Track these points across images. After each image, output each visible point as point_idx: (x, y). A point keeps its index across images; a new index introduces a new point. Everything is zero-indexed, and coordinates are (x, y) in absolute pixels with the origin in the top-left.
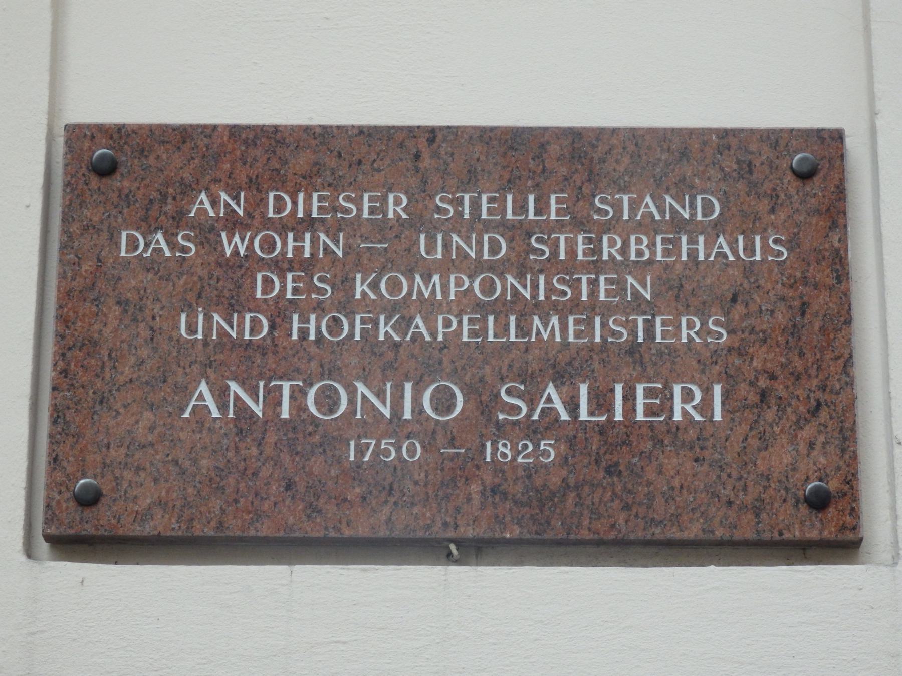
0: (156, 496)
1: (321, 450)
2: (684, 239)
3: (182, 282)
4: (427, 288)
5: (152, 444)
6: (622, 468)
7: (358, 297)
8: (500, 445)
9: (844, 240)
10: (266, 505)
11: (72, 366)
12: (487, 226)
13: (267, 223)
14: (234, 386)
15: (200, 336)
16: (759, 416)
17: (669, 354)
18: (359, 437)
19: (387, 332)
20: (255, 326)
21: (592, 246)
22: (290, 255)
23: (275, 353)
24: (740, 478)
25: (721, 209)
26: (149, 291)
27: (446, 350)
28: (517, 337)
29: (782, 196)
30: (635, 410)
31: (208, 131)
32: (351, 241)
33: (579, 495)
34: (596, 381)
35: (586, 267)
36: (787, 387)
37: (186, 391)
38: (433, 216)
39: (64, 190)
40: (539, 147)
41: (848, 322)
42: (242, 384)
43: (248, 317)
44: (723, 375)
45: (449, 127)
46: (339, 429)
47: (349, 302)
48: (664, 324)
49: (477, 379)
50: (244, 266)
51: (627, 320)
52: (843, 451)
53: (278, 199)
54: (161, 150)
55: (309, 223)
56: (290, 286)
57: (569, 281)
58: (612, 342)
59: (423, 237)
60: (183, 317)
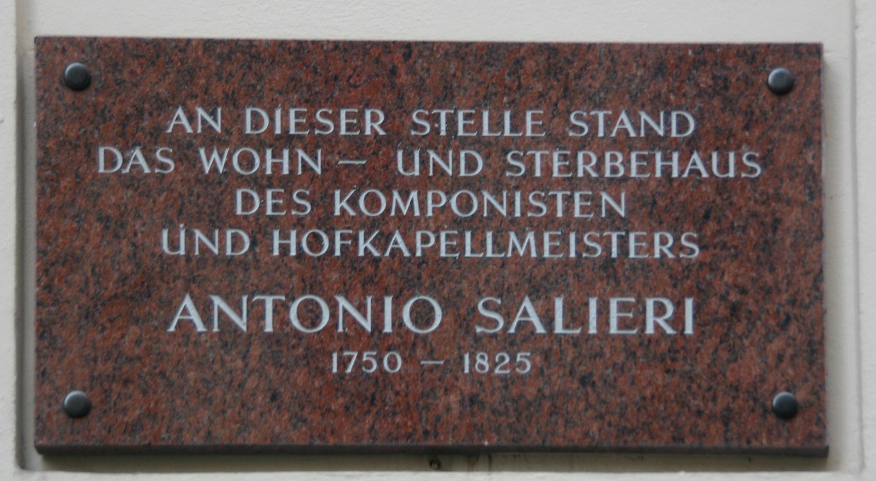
0: (145, 408)
1: (304, 362)
2: (658, 156)
3: (162, 198)
4: (405, 204)
5: (139, 358)
6: (595, 378)
7: (337, 213)
8: (478, 357)
9: (818, 157)
10: (253, 415)
12: (464, 143)
13: (246, 140)
15: (182, 252)
16: (729, 329)
17: (642, 269)
18: (341, 350)
19: (366, 249)
20: (237, 242)
21: (567, 163)
22: (269, 172)
23: (257, 268)
24: (710, 389)
25: (696, 126)
26: (129, 208)
27: (424, 265)
28: (493, 252)
33: (554, 406)
34: (570, 295)
35: (560, 183)
36: (757, 301)
37: (171, 307)
38: (409, 132)
39: (38, 105)
40: (515, 63)
42: (226, 298)
43: (229, 233)
44: (696, 291)
45: (424, 43)
46: (322, 342)
47: (328, 219)
48: (637, 239)
49: (455, 293)
50: (226, 181)
51: (601, 235)
53: (254, 115)
56: (270, 202)
57: (544, 198)
58: (586, 258)
59: (400, 154)
60: (165, 234)
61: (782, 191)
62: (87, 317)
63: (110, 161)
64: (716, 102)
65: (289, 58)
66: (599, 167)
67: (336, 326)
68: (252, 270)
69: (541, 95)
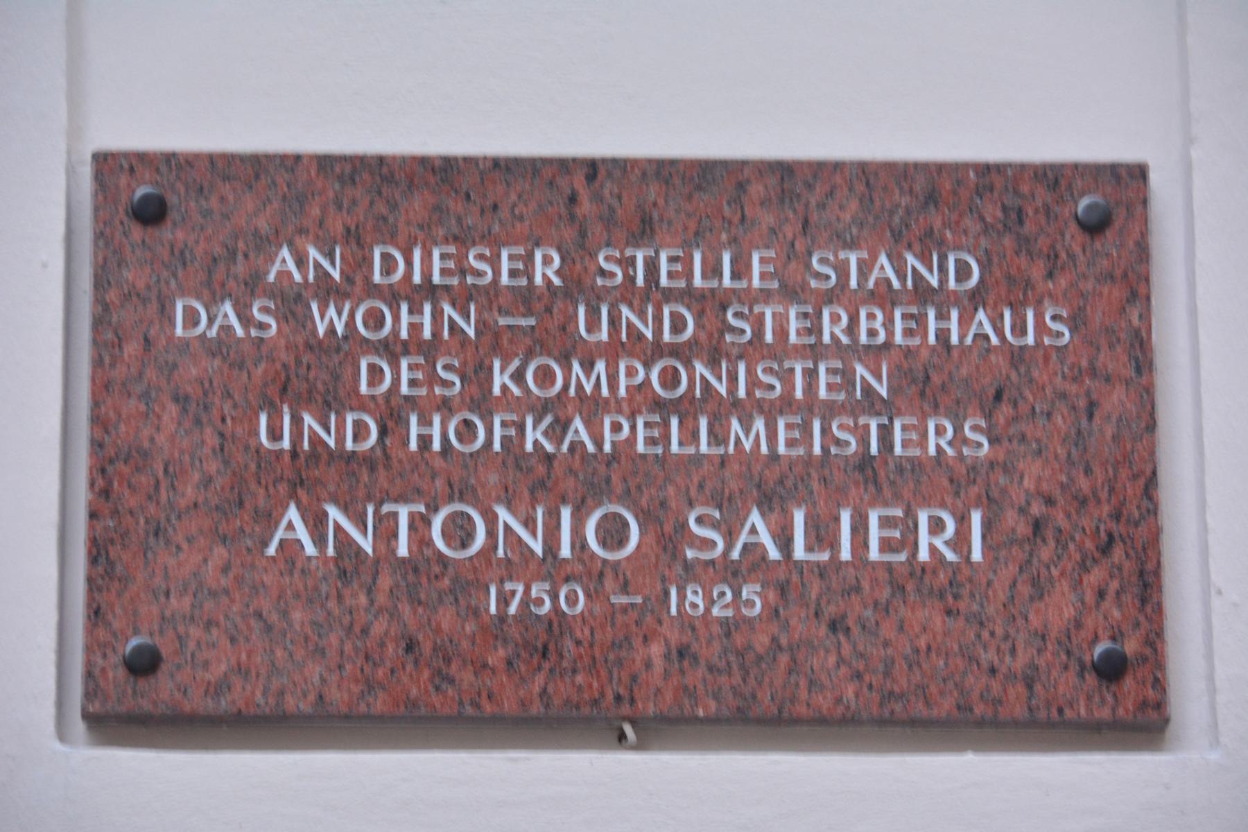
0: (233, 661)
2: (931, 314)
3: (260, 371)
5: (227, 592)
7: (497, 391)
9: (1146, 316)
11: (116, 484)
13: (373, 290)
15: (286, 444)
16: (1031, 555)
18: (502, 581)
19: (536, 442)
20: (360, 431)
22: (404, 334)
23: (388, 467)
24: (1006, 637)
29: (1063, 255)
30: (868, 547)
31: (289, 163)
32: (486, 315)
35: (800, 352)
36: (1068, 516)
37: (270, 519)
42: (345, 509)
43: (349, 419)
44: (984, 500)
46: (475, 569)
48: (904, 428)
50: (344, 348)
52: (1144, 601)
53: (386, 257)
55: (430, 291)
56: (405, 375)
59: (582, 311)
60: (263, 419)
66: (852, 329)
68: (380, 467)
69: (773, 231)
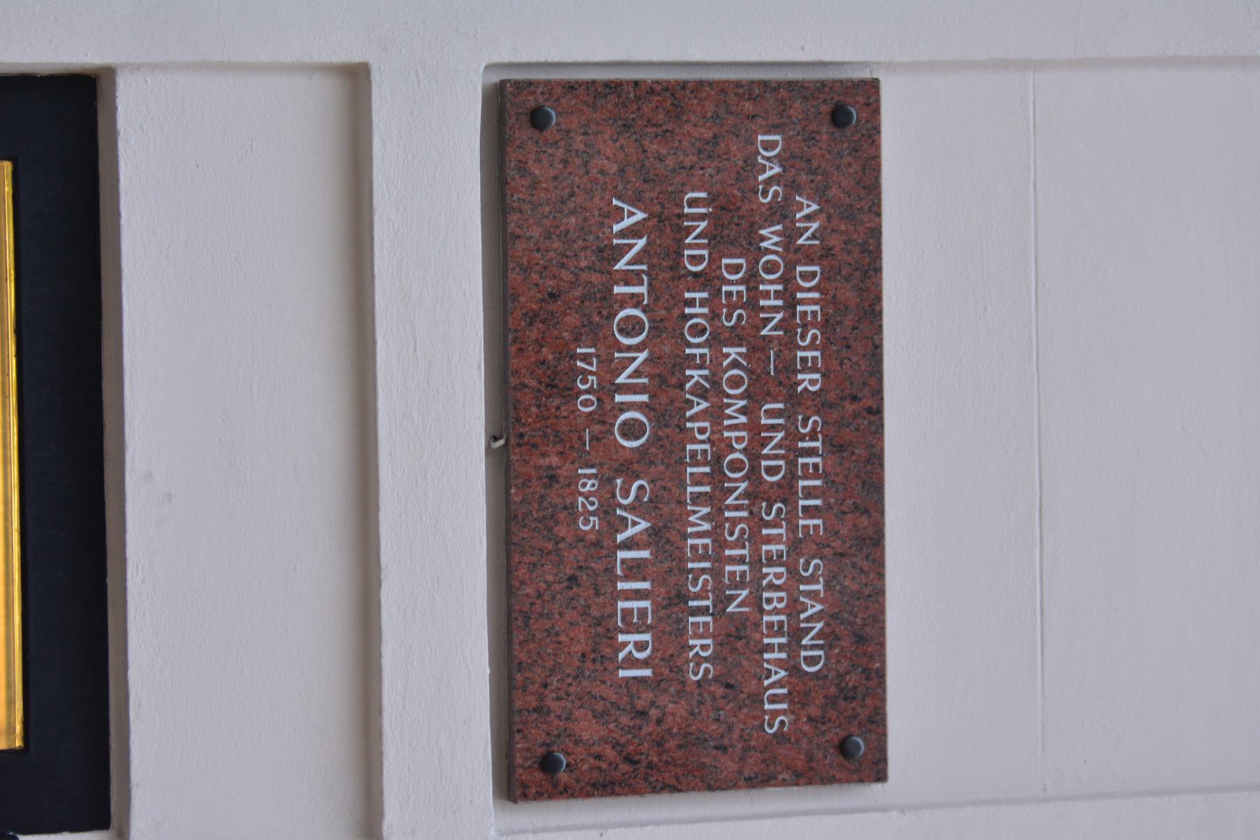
2: (783, 640)
3: (735, 192)
5: (587, 173)
7: (725, 350)
9: (784, 783)
10: (535, 276)
12: (792, 464)
13: (790, 267)
14: (641, 243)
15: (686, 210)
17: (678, 629)
18: (598, 356)
20: (696, 260)
22: (762, 287)
23: (673, 278)
24: (568, 694)
29: (824, 728)
31: (875, 209)
33: (549, 553)
35: (756, 552)
36: (650, 734)
37: (636, 201)
41: (711, 788)
42: (644, 250)
43: (705, 252)
45: (882, 426)
46: (605, 338)
48: (706, 624)
50: (753, 249)
52: (594, 785)
53: (814, 274)
54: (856, 167)
55: (791, 304)
56: (734, 288)
59: (781, 406)
60: (703, 195)
61: (752, 752)
62: (625, 126)
63: (769, 146)
64: (833, 690)
65: (866, 305)
66: (771, 587)
67: (620, 351)
